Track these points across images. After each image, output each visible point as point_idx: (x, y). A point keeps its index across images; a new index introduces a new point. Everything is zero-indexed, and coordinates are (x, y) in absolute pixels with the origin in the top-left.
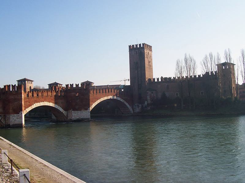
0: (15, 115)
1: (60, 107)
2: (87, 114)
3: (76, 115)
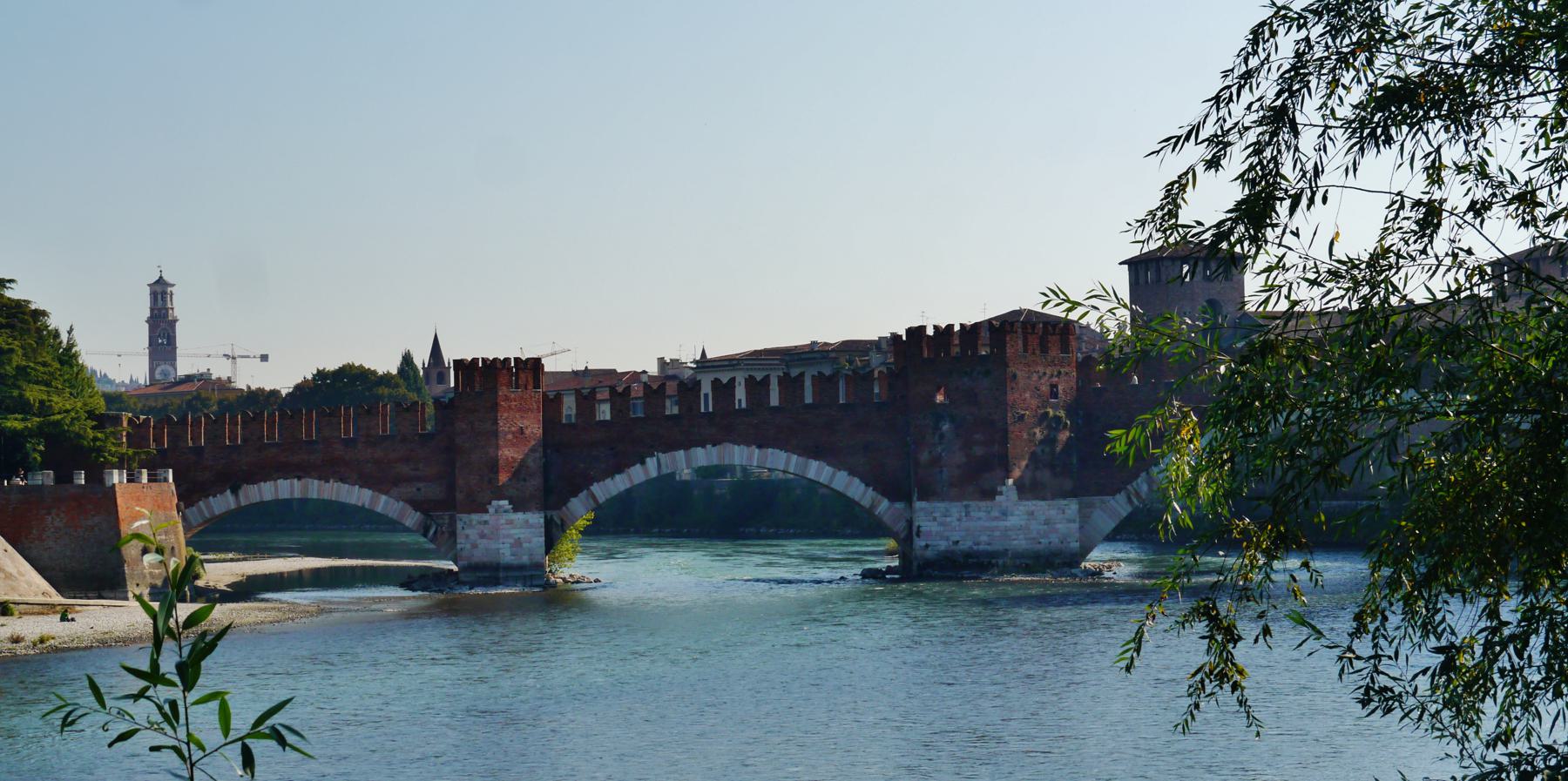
0: (475, 517)
1: (852, 473)
2: (994, 524)
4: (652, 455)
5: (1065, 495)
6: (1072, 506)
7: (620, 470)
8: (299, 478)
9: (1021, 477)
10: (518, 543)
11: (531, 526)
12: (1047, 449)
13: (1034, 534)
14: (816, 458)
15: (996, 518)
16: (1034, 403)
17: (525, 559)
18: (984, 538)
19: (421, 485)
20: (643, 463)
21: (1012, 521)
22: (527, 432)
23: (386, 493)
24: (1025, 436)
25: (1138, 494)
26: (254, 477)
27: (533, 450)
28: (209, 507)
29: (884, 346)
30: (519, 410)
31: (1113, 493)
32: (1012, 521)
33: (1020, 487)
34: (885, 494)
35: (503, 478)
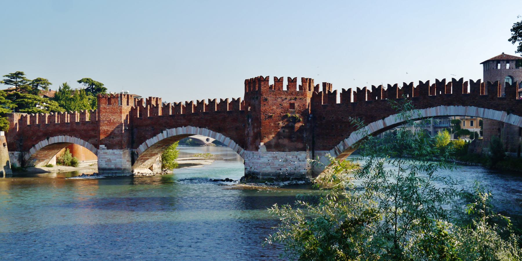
1: (231, 138)
4: (165, 130)
5: (298, 150)
7: (155, 136)
8: (64, 135)
9: (270, 142)
10: (109, 160)
11: (116, 155)
12: (287, 130)
13: (277, 166)
14: (219, 132)
15: (258, 159)
16: (279, 111)
17: (113, 166)
18: (256, 167)
20: (162, 133)
21: (262, 160)
23: (87, 141)
24: (272, 125)
26: (53, 134)
27: (117, 127)
28: (42, 144)
31: (329, 149)
32: (262, 160)
33: (269, 147)
34: (243, 147)
35: (102, 137)
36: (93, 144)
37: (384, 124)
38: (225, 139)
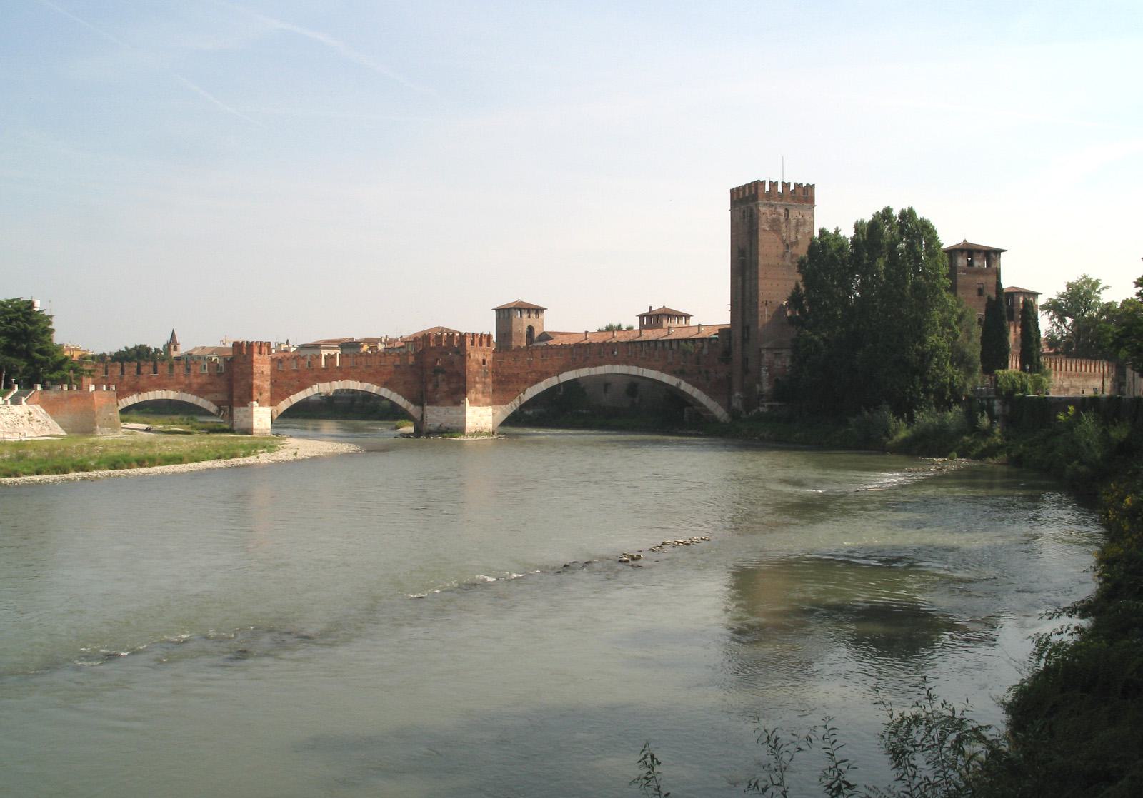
0: (242, 408)
3: (434, 417)
5: (487, 405)
6: (490, 410)
8: (165, 390)
19: (217, 394)
22: (265, 373)
23: (202, 397)
25: (516, 406)
28: (126, 402)
29: (383, 341)
30: (262, 364)
36: (212, 401)
37: (559, 380)
38: (391, 394)
